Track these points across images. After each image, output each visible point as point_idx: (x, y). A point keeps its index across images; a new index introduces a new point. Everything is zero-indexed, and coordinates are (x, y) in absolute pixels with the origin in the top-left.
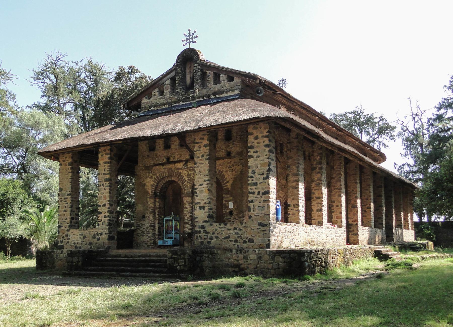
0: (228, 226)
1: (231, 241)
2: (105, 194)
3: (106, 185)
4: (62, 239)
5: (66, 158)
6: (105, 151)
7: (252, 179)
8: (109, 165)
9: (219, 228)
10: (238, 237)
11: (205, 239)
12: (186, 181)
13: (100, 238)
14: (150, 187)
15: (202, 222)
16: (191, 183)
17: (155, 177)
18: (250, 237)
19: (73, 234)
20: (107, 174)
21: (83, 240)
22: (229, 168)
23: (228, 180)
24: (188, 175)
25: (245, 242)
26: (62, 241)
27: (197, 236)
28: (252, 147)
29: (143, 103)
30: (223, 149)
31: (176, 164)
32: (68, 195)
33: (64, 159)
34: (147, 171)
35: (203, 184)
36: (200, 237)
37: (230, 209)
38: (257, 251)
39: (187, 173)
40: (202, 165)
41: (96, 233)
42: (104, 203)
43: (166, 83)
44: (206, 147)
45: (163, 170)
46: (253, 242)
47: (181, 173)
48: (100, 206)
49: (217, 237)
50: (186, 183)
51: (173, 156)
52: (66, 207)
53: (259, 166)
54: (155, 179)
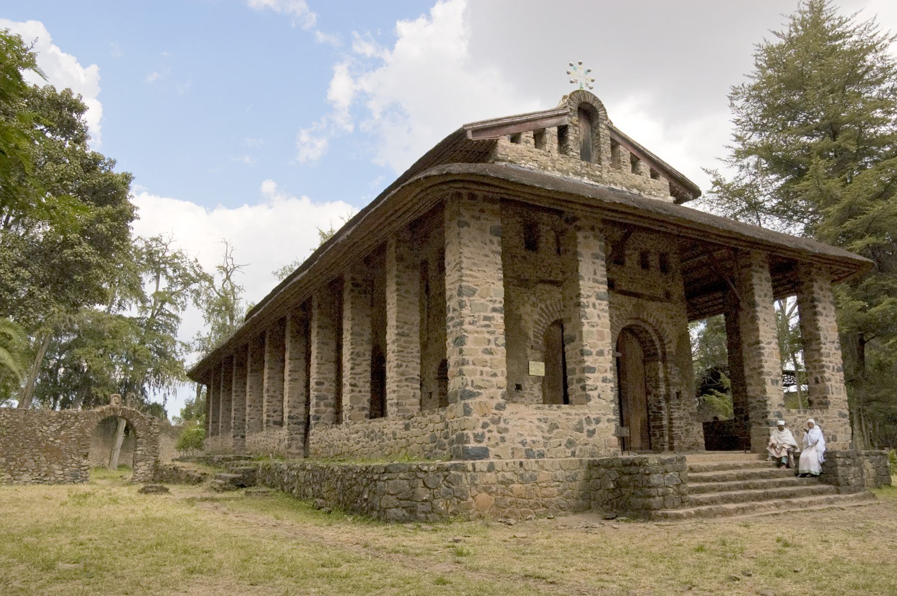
3: (601, 307)
4: (479, 430)
6: (593, 229)
14: (530, 324)
17: (543, 306)
19: (517, 417)
21: (547, 435)
26: (483, 436)
29: (503, 146)
32: (494, 310)
34: (523, 289)
41: (584, 418)
52: (489, 341)
54: (542, 309)
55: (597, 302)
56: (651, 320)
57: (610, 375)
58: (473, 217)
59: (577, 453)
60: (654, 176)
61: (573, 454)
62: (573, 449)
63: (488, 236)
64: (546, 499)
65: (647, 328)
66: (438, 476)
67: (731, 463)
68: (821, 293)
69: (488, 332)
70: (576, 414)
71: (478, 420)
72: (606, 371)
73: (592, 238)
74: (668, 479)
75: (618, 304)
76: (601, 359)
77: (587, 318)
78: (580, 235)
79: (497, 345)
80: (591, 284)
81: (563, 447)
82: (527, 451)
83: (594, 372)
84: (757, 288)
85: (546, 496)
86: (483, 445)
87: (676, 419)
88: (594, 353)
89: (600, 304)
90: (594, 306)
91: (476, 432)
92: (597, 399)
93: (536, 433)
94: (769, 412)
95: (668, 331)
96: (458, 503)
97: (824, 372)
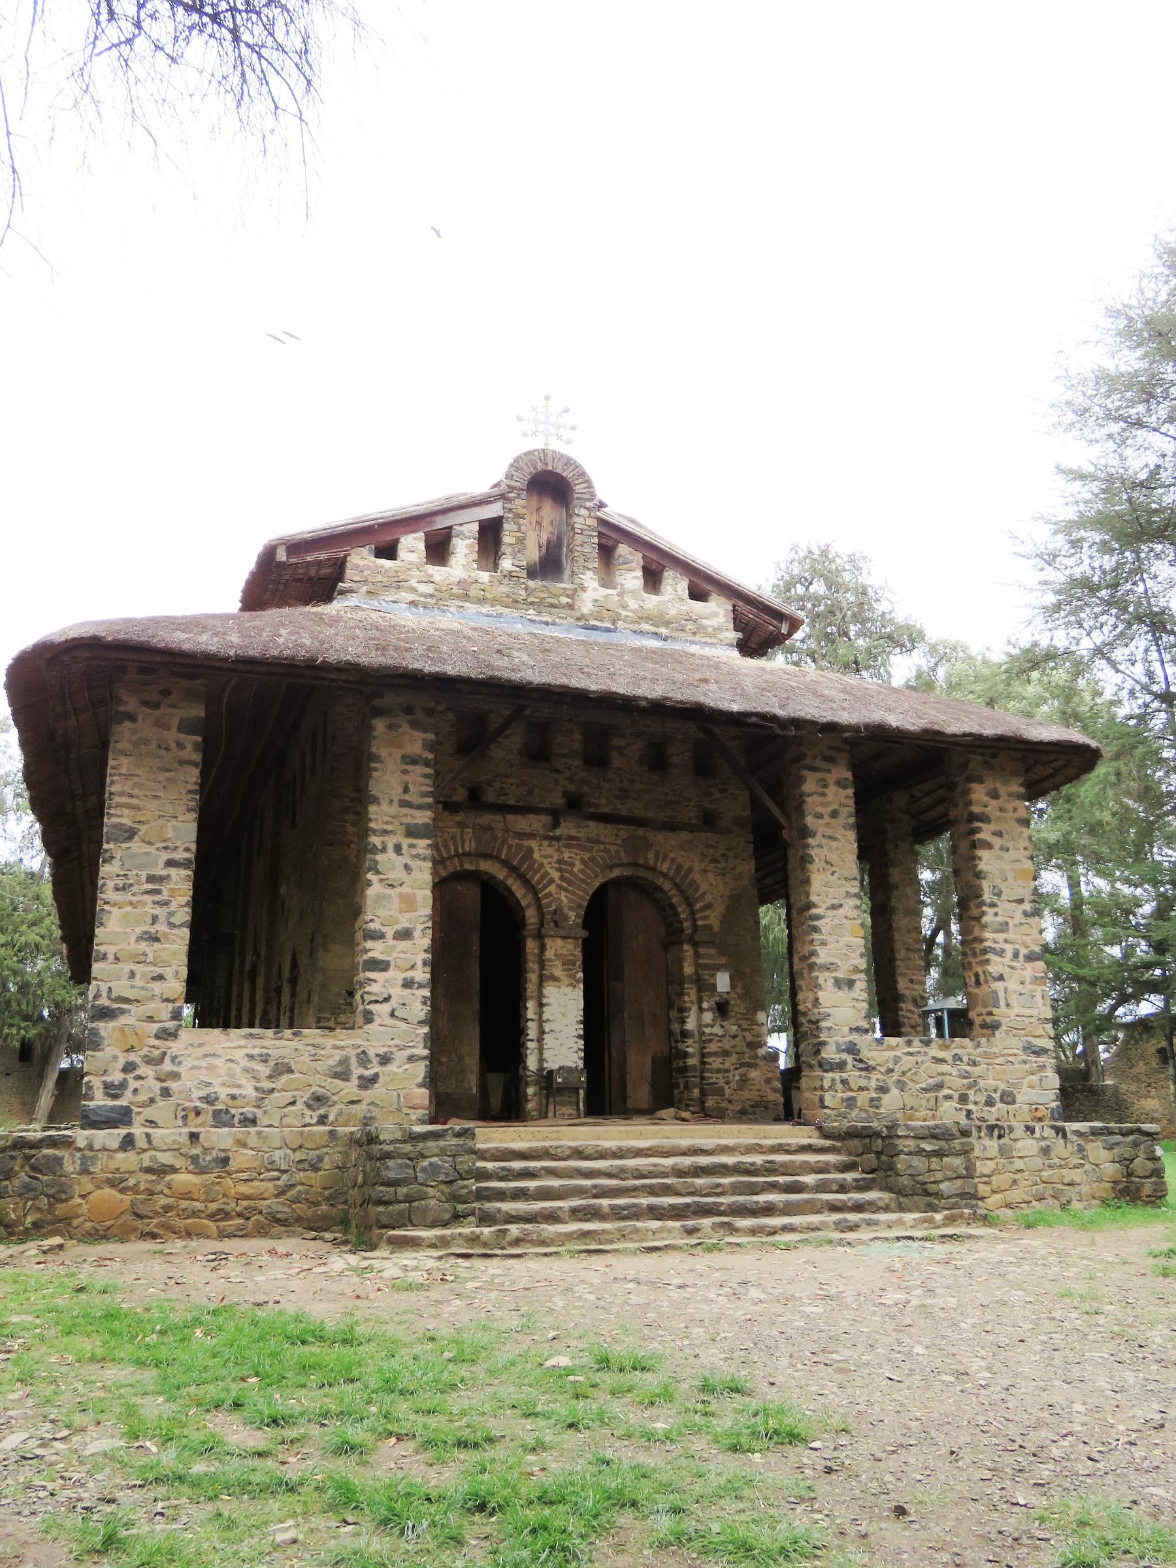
0: (934, 1051)
1: (948, 1097)
2: (406, 889)
3: (414, 851)
4: (116, 1077)
5: (166, 693)
6: (409, 710)
7: (996, 910)
8: (429, 771)
9: (910, 1054)
10: (970, 1087)
11: (861, 1089)
12: (552, 881)
13: (376, 1075)
15: (846, 1030)
16: (574, 894)
18: (1003, 1086)
20: (420, 807)
21: (267, 1085)
22: (712, 861)
23: (709, 898)
24: (559, 862)
25: (990, 1103)
26: (123, 1085)
27: (833, 1080)
28: (985, 819)
29: (357, 566)
30: (688, 800)
31: (510, 818)
32: (170, 863)
33: (154, 697)
35: (841, 906)
36: (844, 1082)
37: (720, 994)
38: (1037, 1129)
39: (556, 856)
40: (834, 844)
41: (354, 1052)
42: (407, 925)
43: (464, 528)
44: (844, 787)
45: (458, 831)
46: (1014, 1102)
47: (530, 851)
48: (380, 936)
49: (901, 1086)
50: (552, 888)
51: (497, 785)
53: (1010, 876)
55: (405, 842)
56: (665, 868)
57: (422, 975)
58: (145, 703)
59: (331, 1118)
60: (697, 594)
61: (322, 1120)
62: (322, 1111)
63: (172, 736)
64: (245, 1203)
65: (660, 881)
66: (13, 1158)
67: (685, 1143)
68: (993, 803)
69: (155, 903)
70: (336, 1047)
71: (115, 1057)
72: (412, 967)
73: (406, 727)
74: (424, 1170)
75: (589, 840)
76: (403, 945)
77: (378, 872)
78: (380, 726)
79: (172, 925)
80: (394, 809)
81: (300, 1106)
82: (217, 1114)
83: (385, 970)
84: (813, 804)
85: (247, 1198)
86: (122, 1102)
87: (715, 1054)
88: (389, 932)
89: (411, 846)
90: (398, 849)
91: (109, 1079)
92: (389, 1021)
93: (243, 1082)
94: (824, 1043)
95: (704, 887)
96: (50, 1205)
97: (987, 962)
